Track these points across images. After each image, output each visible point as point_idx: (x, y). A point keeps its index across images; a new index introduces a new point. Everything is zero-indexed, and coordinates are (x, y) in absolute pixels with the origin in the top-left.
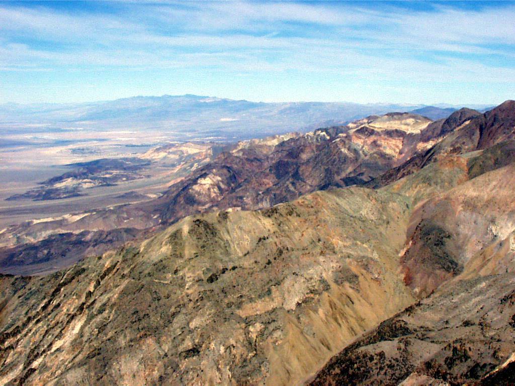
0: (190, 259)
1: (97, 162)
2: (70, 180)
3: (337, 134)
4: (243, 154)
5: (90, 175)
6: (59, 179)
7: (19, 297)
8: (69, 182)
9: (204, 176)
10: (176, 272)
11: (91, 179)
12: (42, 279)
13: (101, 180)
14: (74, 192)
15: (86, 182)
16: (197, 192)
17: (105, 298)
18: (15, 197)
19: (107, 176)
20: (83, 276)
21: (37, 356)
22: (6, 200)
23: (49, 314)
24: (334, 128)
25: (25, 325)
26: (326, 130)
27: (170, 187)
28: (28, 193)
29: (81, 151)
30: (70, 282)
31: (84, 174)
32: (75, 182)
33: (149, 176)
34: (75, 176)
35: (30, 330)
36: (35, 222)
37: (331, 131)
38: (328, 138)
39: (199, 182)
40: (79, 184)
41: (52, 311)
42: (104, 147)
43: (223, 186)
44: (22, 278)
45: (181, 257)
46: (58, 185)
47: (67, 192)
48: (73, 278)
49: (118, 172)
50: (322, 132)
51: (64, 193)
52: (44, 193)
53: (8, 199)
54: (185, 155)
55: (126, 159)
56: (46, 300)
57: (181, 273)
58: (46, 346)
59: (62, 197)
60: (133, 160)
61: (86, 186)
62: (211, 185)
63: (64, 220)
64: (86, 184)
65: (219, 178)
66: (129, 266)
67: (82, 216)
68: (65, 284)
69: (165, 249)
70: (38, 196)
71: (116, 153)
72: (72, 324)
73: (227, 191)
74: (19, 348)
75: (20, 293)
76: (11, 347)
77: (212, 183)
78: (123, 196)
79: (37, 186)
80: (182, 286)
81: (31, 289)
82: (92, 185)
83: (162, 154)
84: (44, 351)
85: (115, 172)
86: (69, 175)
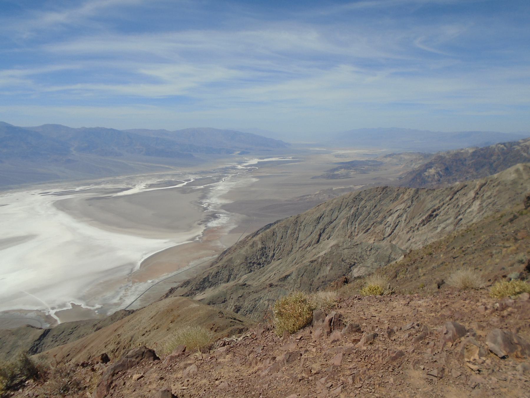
0: (527, 180)
1: (352, 162)
2: (343, 170)
3: (511, 146)
4: (452, 157)
7: (431, 197)
8: (342, 171)
9: (431, 168)
10: (522, 184)
11: (355, 170)
12: (441, 190)
14: (347, 176)
15: (352, 171)
16: (427, 176)
17: (489, 193)
18: (313, 178)
19: (362, 168)
20: (466, 188)
21: (460, 215)
22: (312, 178)
23: (453, 202)
24: (509, 143)
25: (442, 206)
26: (504, 144)
27: (400, 175)
28: (322, 175)
30: (461, 190)
32: (346, 171)
33: (386, 170)
34: (345, 168)
35: (446, 208)
36: (334, 189)
37: (507, 145)
38: (505, 148)
39: (427, 170)
40: (348, 172)
41: (455, 200)
43: (441, 173)
44: (430, 190)
45: (522, 178)
46: (336, 173)
47: (343, 176)
48: (462, 188)
49: (368, 167)
50: (501, 145)
54: (403, 159)
55: (369, 161)
56: (450, 197)
57: (524, 185)
58: (463, 211)
60: (373, 161)
62: (436, 172)
64: (352, 173)
65: (439, 169)
66: (495, 182)
67: (361, 186)
68: (458, 191)
69: (514, 176)
72: (474, 203)
73: (444, 176)
74: (441, 214)
75: (431, 195)
76: (437, 215)
77: (436, 171)
78: (375, 179)
80: (526, 190)
81: (437, 193)
83: (388, 159)
84: (463, 213)
85: (366, 167)
86: (341, 168)
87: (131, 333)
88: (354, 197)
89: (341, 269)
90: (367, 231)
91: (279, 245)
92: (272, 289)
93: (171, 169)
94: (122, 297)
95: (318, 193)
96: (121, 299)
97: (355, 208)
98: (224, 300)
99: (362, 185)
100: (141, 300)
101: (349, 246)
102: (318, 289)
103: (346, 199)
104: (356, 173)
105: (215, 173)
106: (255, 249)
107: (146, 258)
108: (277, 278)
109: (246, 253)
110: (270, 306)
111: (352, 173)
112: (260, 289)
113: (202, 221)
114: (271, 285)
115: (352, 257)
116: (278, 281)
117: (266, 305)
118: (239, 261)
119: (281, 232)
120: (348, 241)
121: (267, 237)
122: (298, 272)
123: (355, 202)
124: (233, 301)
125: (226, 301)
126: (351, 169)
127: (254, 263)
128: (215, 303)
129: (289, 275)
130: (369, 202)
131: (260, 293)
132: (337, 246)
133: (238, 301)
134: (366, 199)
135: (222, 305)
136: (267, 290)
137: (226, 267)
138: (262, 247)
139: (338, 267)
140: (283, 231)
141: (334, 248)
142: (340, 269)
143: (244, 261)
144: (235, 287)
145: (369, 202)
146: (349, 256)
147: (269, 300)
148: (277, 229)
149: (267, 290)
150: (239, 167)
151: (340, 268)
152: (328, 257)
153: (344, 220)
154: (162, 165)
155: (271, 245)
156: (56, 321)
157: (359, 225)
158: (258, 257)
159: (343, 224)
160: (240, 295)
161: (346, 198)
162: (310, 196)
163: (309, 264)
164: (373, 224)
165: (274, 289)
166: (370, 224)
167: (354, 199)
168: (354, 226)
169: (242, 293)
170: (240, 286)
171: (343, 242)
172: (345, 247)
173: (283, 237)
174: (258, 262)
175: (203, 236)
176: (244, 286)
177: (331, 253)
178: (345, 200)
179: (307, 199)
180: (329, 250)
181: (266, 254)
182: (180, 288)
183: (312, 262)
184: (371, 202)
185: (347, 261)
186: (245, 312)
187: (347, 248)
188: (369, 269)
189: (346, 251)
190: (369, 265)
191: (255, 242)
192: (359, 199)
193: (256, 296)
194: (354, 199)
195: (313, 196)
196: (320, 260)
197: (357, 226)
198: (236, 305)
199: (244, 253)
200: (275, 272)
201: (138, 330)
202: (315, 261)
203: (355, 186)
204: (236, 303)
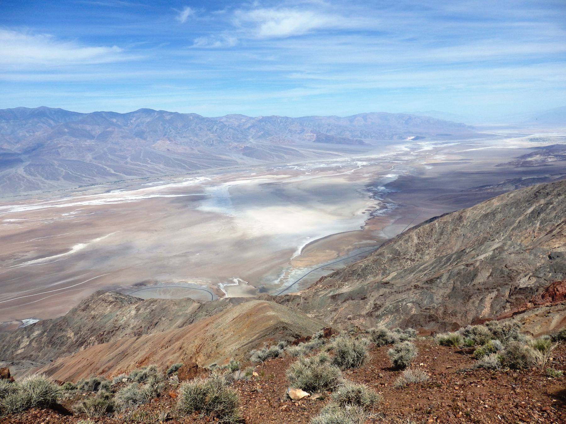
1: (552, 146)
2: (538, 156)
5: (551, 154)
6: (530, 155)
11: (555, 156)
13: (562, 156)
15: (550, 158)
29: (536, 140)
31: (547, 153)
32: (542, 157)
34: (541, 154)
36: (524, 178)
40: (546, 159)
42: (552, 138)
46: (529, 159)
47: (538, 163)
51: (536, 164)
52: (521, 163)
53: (496, 166)
59: (535, 166)
61: (550, 160)
63: (546, 177)
70: (518, 165)
71: (562, 141)
79: (513, 159)
82: (555, 159)
86: (536, 154)
87: (213, 332)
88: (537, 190)
89: (504, 277)
90: (551, 232)
91: (437, 242)
92: (417, 291)
93: (340, 155)
94: (282, 279)
95: (502, 183)
96: (281, 281)
97: (537, 205)
98: (364, 297)
99: (561, 174)
100: (299, 284)
101: (517, 250)
102: (471, 297)
103: (527, 194)
104: (555, 159)
105: (385, 160)
106: (409, 244)
107: (307, 243)
108: (426, 278)
109: (399, 248)
110: (414, 309)
111: (550, 160)
112: (404, 289)
113: (366, 210)
114: (416, 287)
115: (520, 264)
116: (424, 283)
117: (409, 308)
118: (391, 256)
119: (442, 228)
120: (516, 244)
121: (425, 233)
122: (450, 275)
123: (538, 198)
124: (373, 299)
125: (366, 298)
126: (550, 155)
127: (408, 259)
128: (354, 299)
129: (438, 278)
130: (558, 198)
131: (403, 293)
132: (501, 250)
133: (379, 299)
134: (553, 194)
135: (361, 301)
136: (411, 292)
137: (376, 261)
138: (418, 243)
139: (499, 274)
140: (444, 226)
141: (497, 252)
142: (502, 277)
143: (396, 256)
144: (377, 284)
145: (558, 198)
146: (515, 263)
147: (413, 302)
148: (437, 224)
149: (412, 291)
150: (412, 153)
151: (503, 275)
152: (488, 261)
153: (521, 218)
154: (331, 152)
155: (429, 241)
156: (224, 294)
157: (540, 225)
158: (413, 254)
159: (519, 222)
160: (382, 294)
161: (527, 193)
162: (491, 187)
163: (463, 267)
164: (560, 224)
165: (420, 291)
166: (556, 225)
167: (537, 194)
168: (534, 226)
169: (384, 292)
170: (382, 284)
171: (511, 246)
172: (512, 250)
173: (445, 233)
174: (413, 258)
175: (365, 225)
176: (386, 285)
177: (493, 257)
178: (525, 194)
179: (487, 189)
180: (491, 253)
181: (423, 251)
182: (329, 278)
183: (467, 265)
184: (560, 198)
185: (514, 268)
186: (385, 312)
187: (514, 253)
188: (542, 281)
189: (513, 255)
190: (542, 275)
191: (411, 237)
192: (544, 193)
193: (400, 297)
194: (537, 194)
195: (496, 187)
196: (478, 264)
197: (538, 225)
198: (376, 304)
199: (397, 248)
200: (426, 272)
201: (220, 330)
202: (472, 264)
203: (552, 175)
204: (376, 301)
